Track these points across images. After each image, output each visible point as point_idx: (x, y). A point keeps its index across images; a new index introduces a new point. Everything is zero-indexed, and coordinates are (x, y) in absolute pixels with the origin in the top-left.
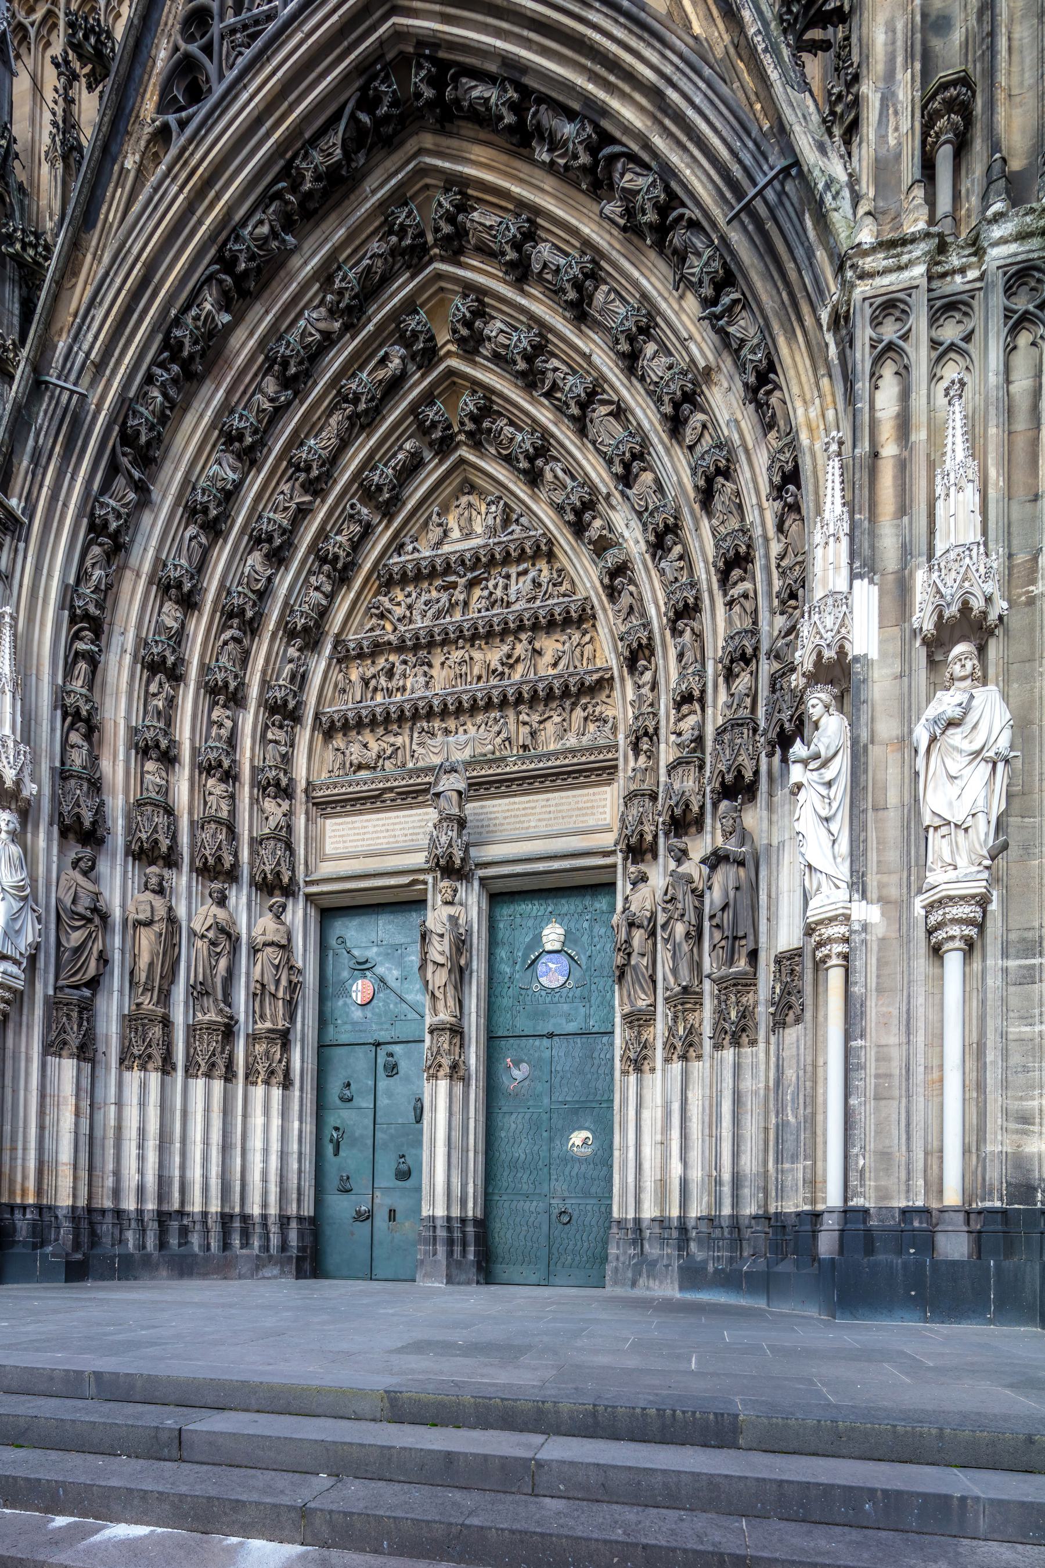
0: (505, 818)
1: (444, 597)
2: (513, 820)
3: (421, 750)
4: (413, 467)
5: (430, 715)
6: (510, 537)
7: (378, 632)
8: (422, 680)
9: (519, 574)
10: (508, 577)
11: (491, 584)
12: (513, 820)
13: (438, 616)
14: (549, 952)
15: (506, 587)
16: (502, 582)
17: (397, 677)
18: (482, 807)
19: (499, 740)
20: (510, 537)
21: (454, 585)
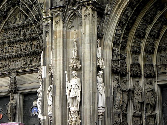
0: (26, 78)
1: (15, 33)
2: (28, 79)
3: (11, 66)
4: (8, 10)
5: (13, 58)
6: (26, 22)
7: (4, 41)
8: (11, 50)
9: (29, 28)
10: (27, 29)
11: (24, 31)
12: (28, 79)
13: (14, 37)
14: (35, 107)
15: (27, 31)
16: (26, 30)
17: (7, 49)
18: (22, 76)
19: (24, 64)
20: (26, 22)
21: (17, 31)
